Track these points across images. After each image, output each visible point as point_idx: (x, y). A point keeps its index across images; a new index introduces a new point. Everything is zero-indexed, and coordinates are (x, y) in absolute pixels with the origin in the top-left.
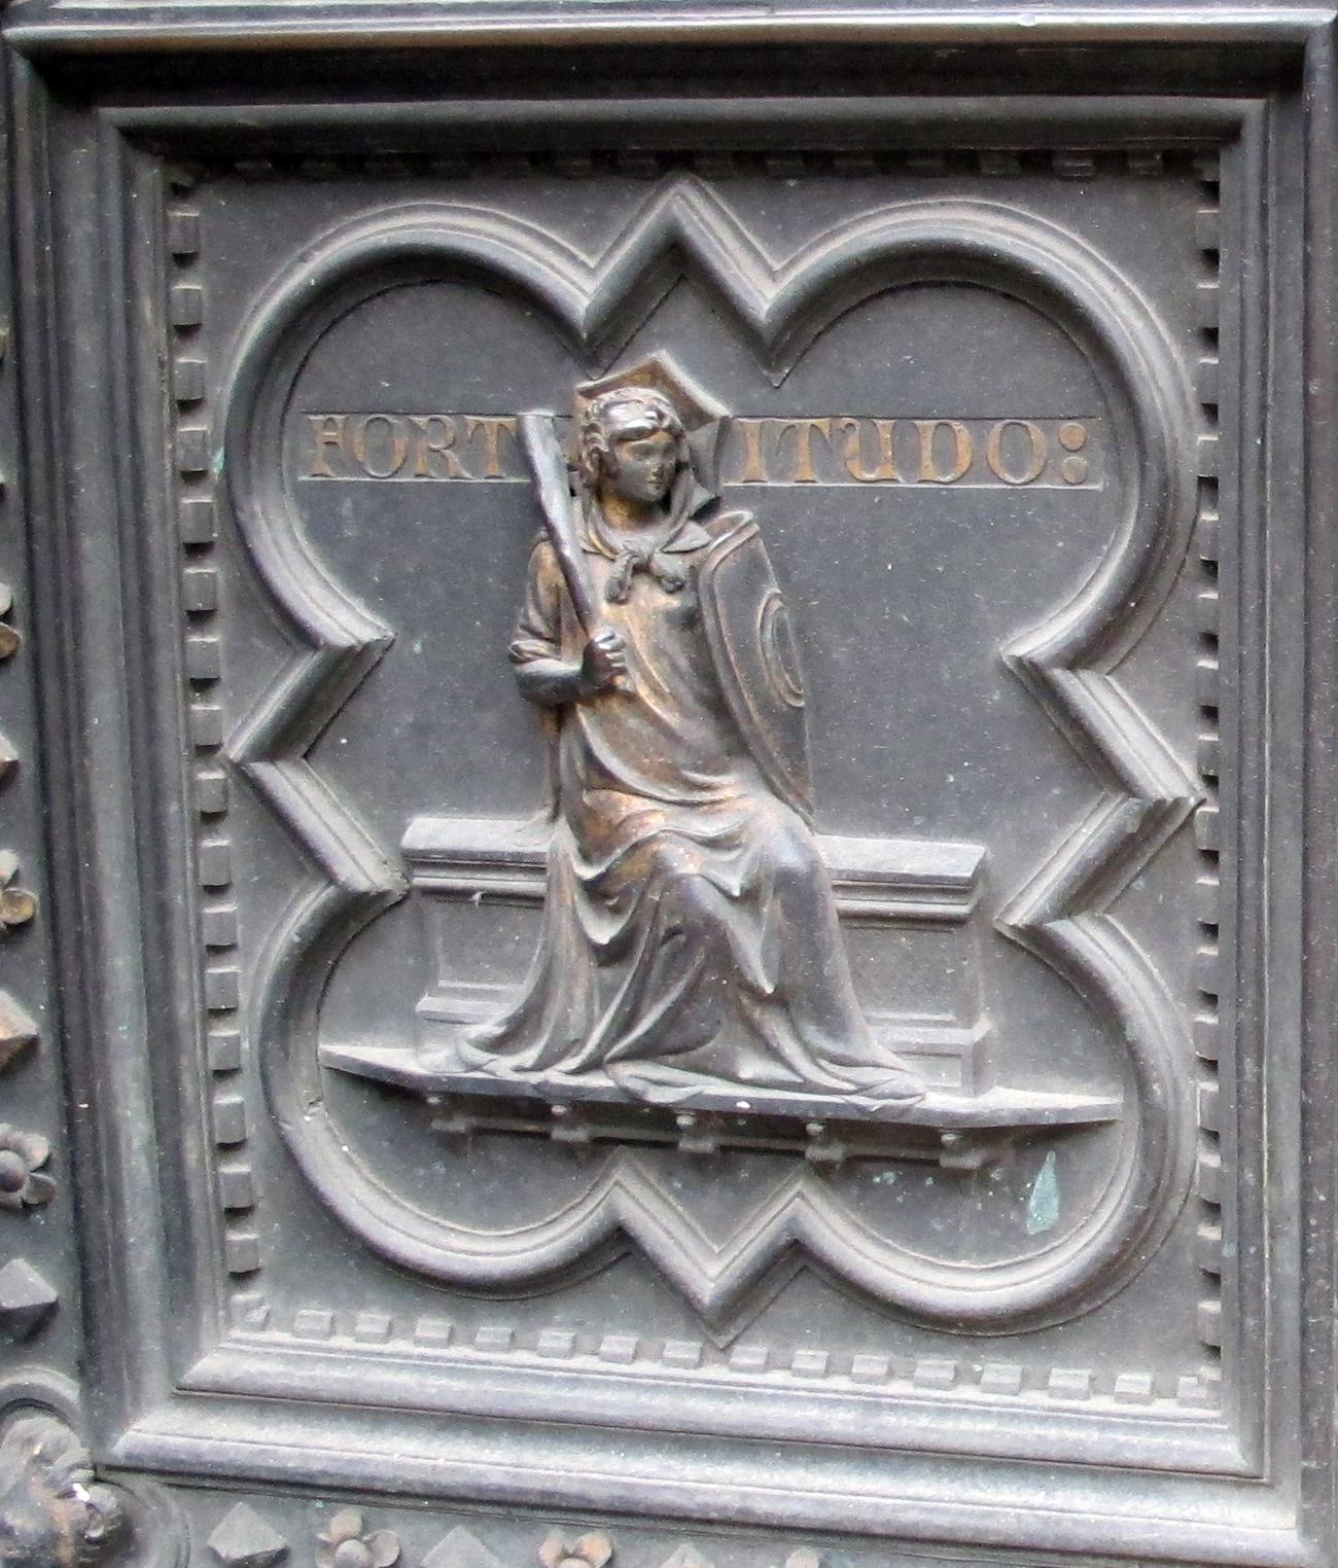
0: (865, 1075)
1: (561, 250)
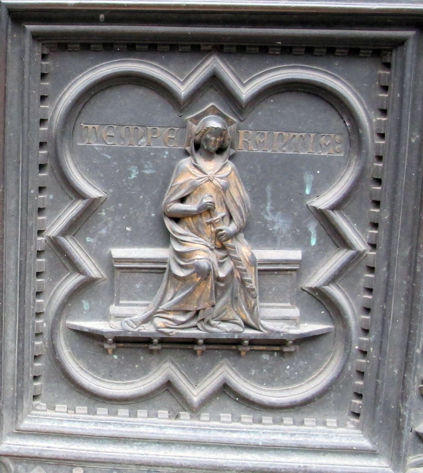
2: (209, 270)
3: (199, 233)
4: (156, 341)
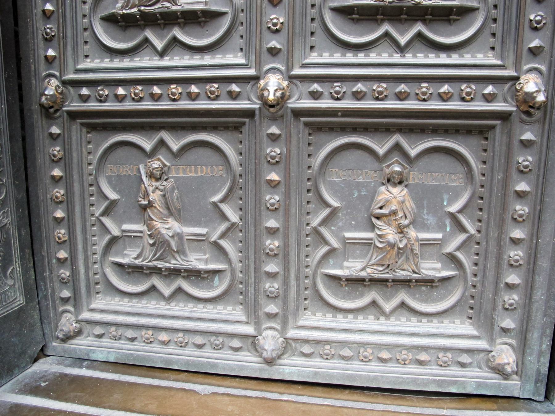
0: (190, 263)
1: (145, 141)
2: (395, 244)
3: (389, 225)
4: (367, 280)
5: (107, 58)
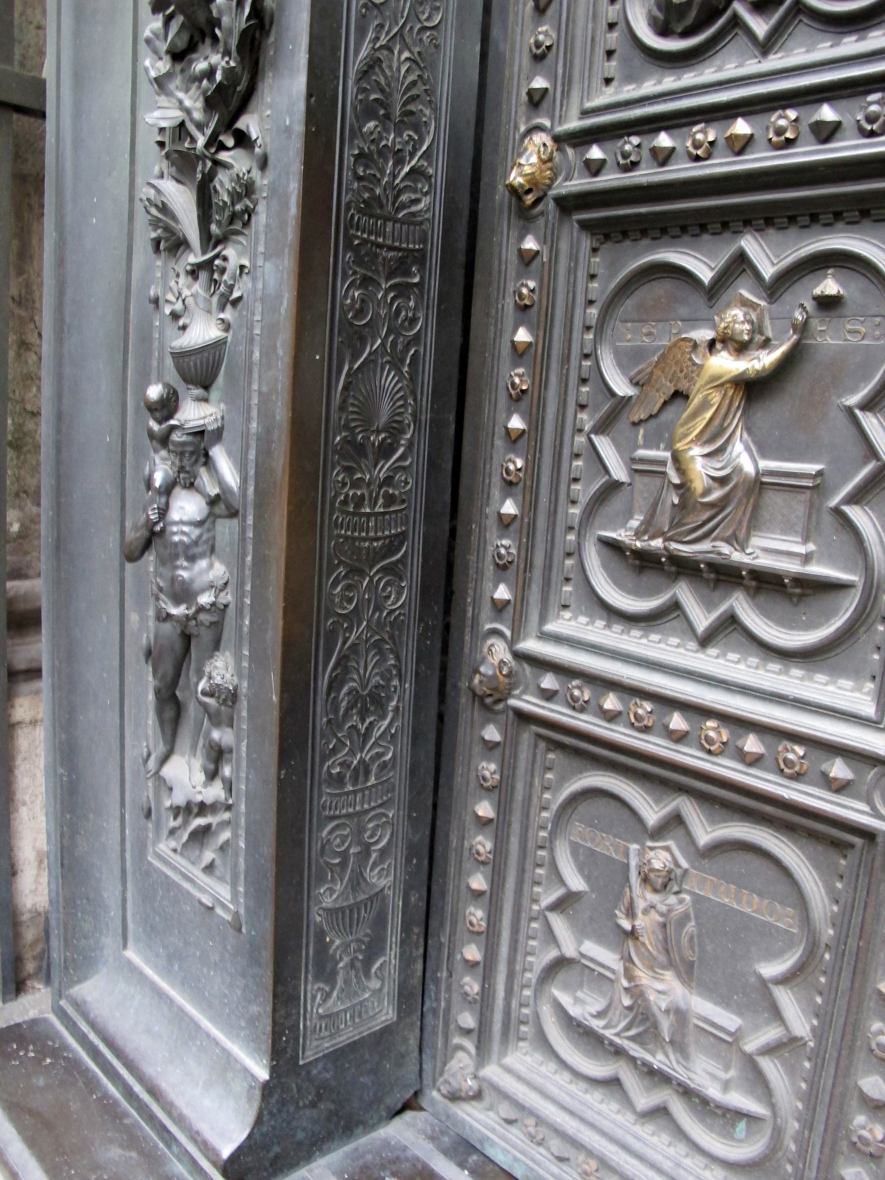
5: (601, 619)
